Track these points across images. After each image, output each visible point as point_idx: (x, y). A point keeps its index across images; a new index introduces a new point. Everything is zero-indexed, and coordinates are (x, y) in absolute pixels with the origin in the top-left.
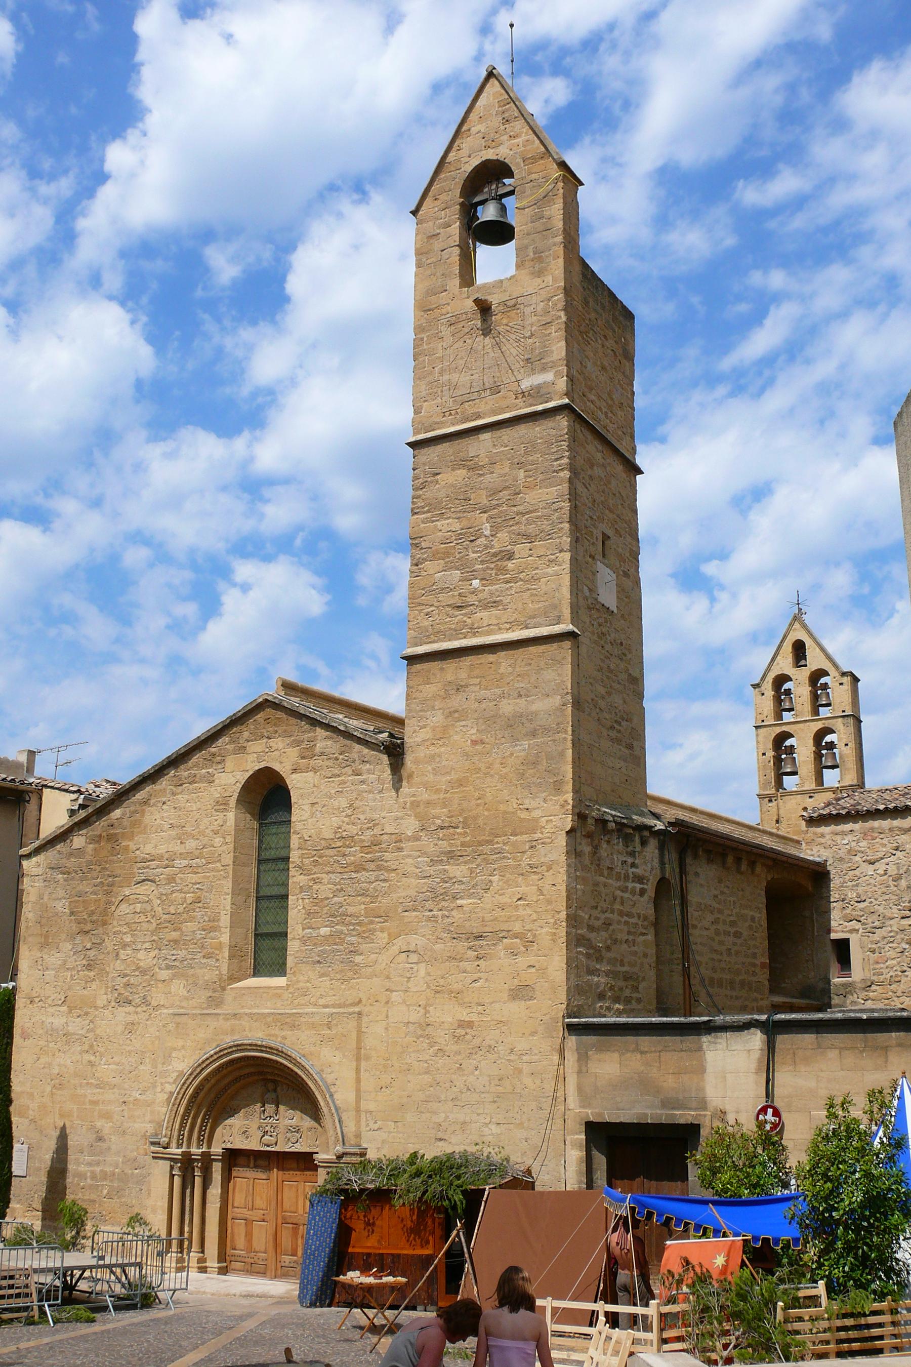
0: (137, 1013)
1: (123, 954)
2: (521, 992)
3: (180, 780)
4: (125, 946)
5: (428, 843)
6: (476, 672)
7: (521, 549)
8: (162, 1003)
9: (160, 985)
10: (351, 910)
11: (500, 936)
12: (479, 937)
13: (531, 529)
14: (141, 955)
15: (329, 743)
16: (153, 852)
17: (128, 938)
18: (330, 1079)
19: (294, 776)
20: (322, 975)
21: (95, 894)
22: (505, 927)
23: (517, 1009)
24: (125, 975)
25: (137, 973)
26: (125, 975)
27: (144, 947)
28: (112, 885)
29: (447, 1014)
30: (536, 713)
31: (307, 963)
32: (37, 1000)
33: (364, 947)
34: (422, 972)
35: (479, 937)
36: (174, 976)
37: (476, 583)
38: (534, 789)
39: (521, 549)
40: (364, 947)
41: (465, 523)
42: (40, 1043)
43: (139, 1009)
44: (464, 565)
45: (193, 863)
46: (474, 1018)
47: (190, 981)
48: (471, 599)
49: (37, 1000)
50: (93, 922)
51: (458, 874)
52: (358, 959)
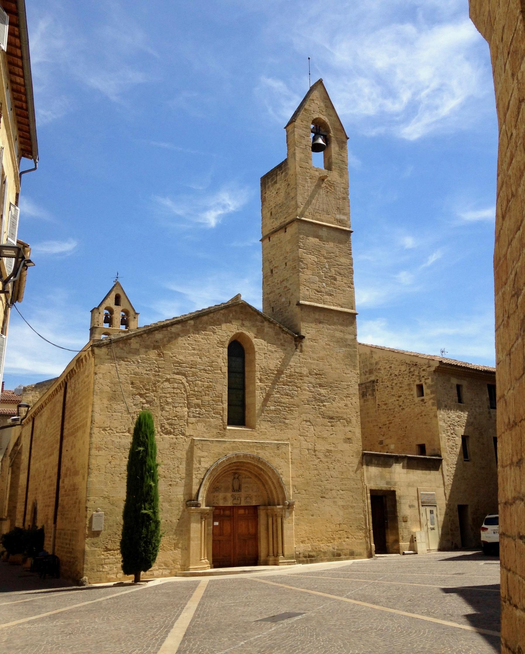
0: (176, 438)
1: (167, 408)
2: (348, 440)
3: (197, 327)
4: (168, 403)
5: (312, 379)
6: (326, 318)
7: (339, 278)
8: (192, 434)
9: (190, 425)
10: (283, 400)
11: (339, 418)
12: (332, 418)
13: (342, 271)
14: (177, 409)
15: (270, 330)
16: (184, 359)
17: (170, 400)
18: (280, 471)
19: (256, 339)
20: (272, 427)
21: (147, 375)
22: (341, 415)
23: (346, 446)
24: (168, 419)
25: (176, 418)
26: (168, 419)
27: (180, 405)
28: (159, 372)
29: (322, 446)
30: (347, 339)
31: (265, 421)
32: (108, 429)
33: (289, 416)
34: (313, 429)
35: (332, 418)
36: (198, 421)
37: (324, 284)
38: (348, 367)
39: (339, 278)
40: (289, 416)
41: (319, 260)
42: (111, 453)
43: (178, 436)
44: (320, 277)
45: (207, 368)
46: (332, 449)
47: (207, 424)
48: (323, 289)
49: (108, 429)
50: (146, 390)
51: (323, 392)
52: (287, 421)
